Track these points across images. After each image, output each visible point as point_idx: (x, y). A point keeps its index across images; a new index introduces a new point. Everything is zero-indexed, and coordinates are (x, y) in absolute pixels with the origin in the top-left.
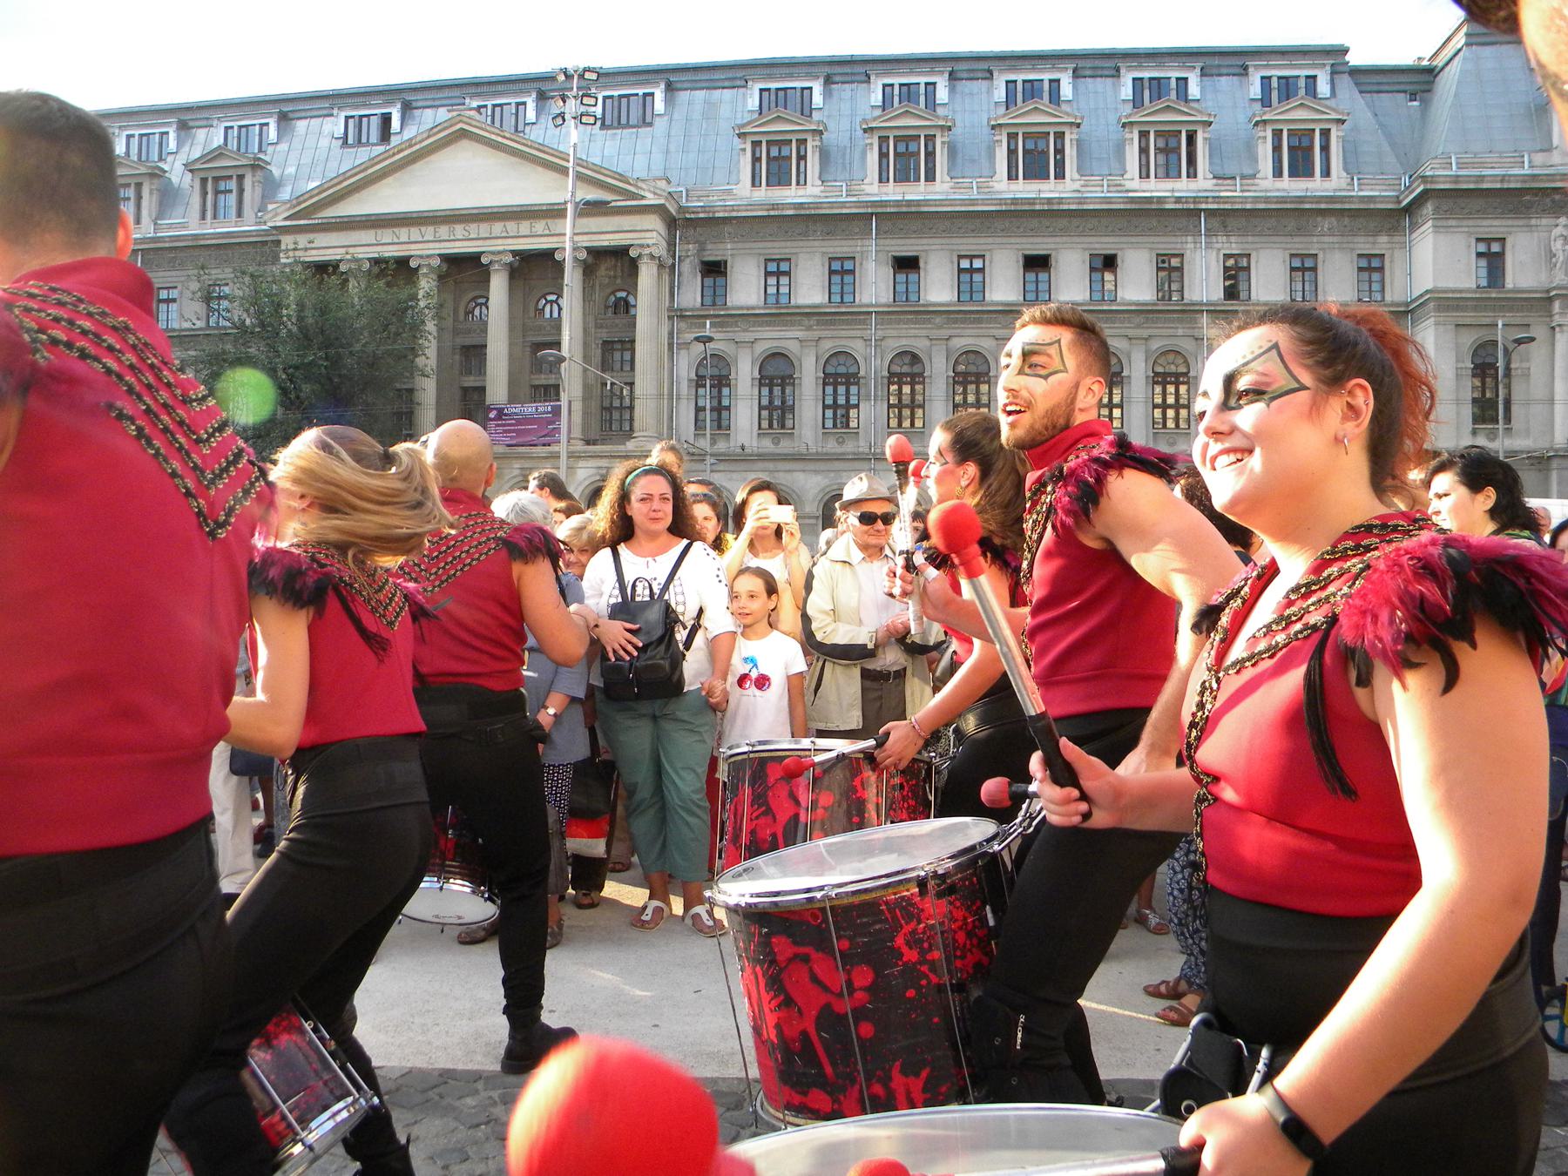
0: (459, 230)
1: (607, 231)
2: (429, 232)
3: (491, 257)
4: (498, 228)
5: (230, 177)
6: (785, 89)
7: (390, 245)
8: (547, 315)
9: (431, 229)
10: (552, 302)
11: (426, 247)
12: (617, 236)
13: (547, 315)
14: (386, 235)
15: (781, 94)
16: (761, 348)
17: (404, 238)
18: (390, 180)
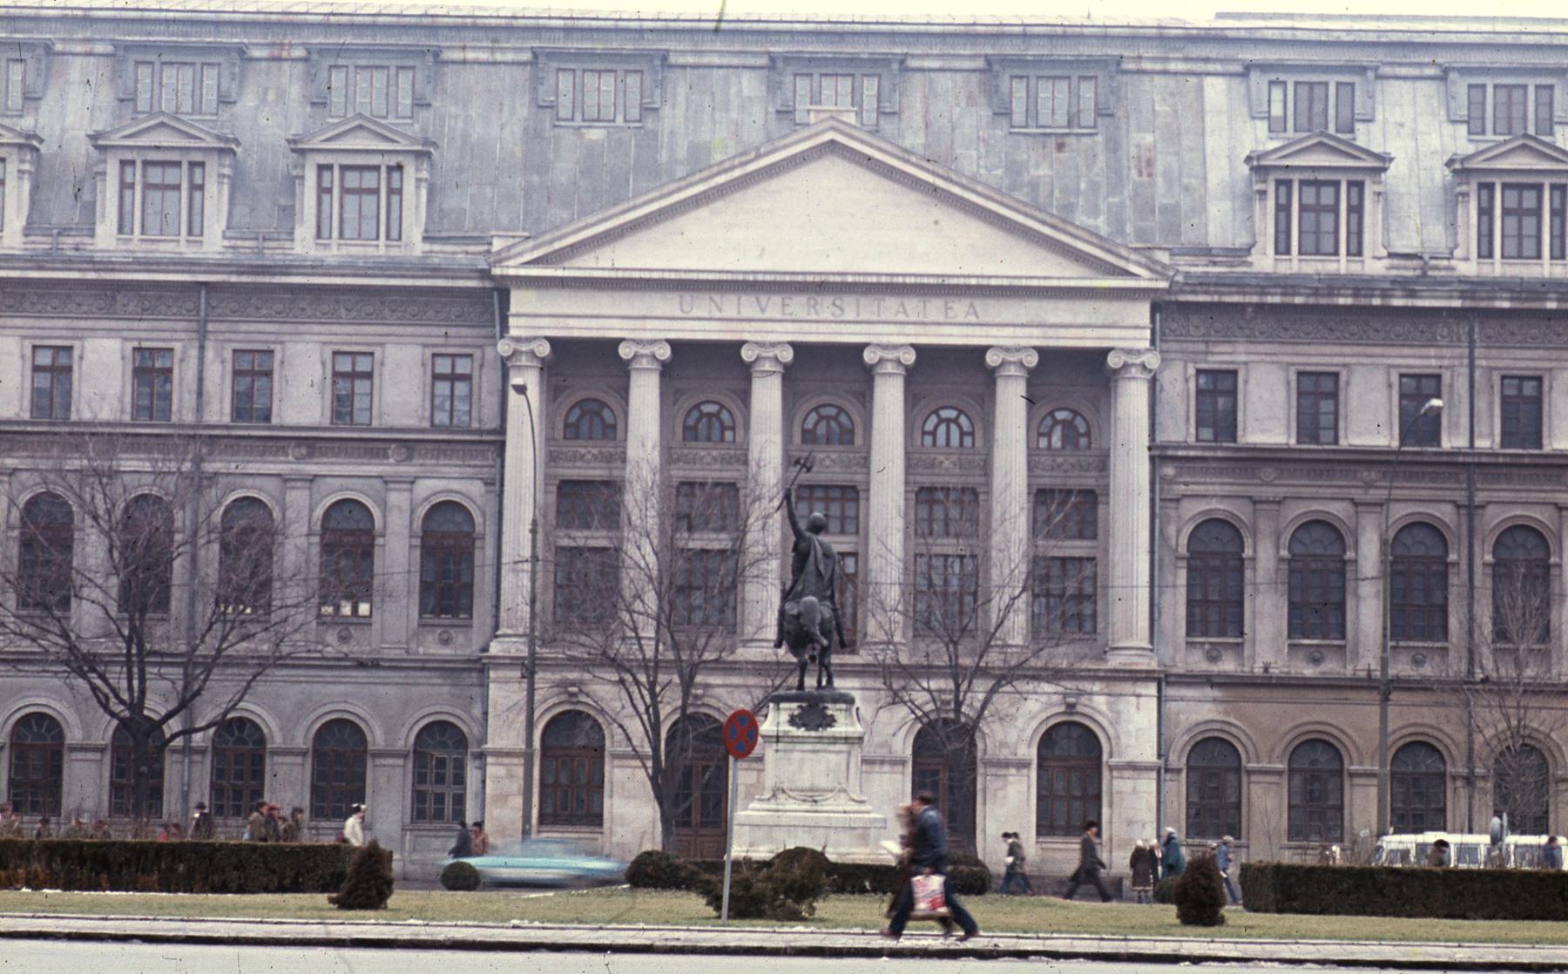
0: (826, 306)
1: (1074, 327)
2: (774, 305)
3: (880, 353)
4: (891, 305)
5: (377, 168)
6: (1311, 85)
7: (705, 322)
8: (941, 440)
9: (777, 299)
10: (948, 421)
11: (769, 330)
12: (1089, 332)
13: (941, 440)
14: (702, 305)
15: (1303, 91)
16: (1295, 512)
17: (729, 312)
18: (703, 212)
